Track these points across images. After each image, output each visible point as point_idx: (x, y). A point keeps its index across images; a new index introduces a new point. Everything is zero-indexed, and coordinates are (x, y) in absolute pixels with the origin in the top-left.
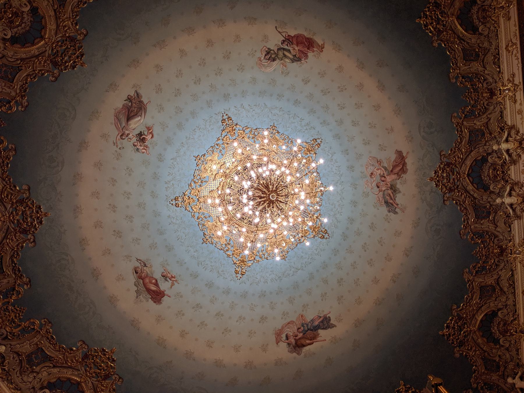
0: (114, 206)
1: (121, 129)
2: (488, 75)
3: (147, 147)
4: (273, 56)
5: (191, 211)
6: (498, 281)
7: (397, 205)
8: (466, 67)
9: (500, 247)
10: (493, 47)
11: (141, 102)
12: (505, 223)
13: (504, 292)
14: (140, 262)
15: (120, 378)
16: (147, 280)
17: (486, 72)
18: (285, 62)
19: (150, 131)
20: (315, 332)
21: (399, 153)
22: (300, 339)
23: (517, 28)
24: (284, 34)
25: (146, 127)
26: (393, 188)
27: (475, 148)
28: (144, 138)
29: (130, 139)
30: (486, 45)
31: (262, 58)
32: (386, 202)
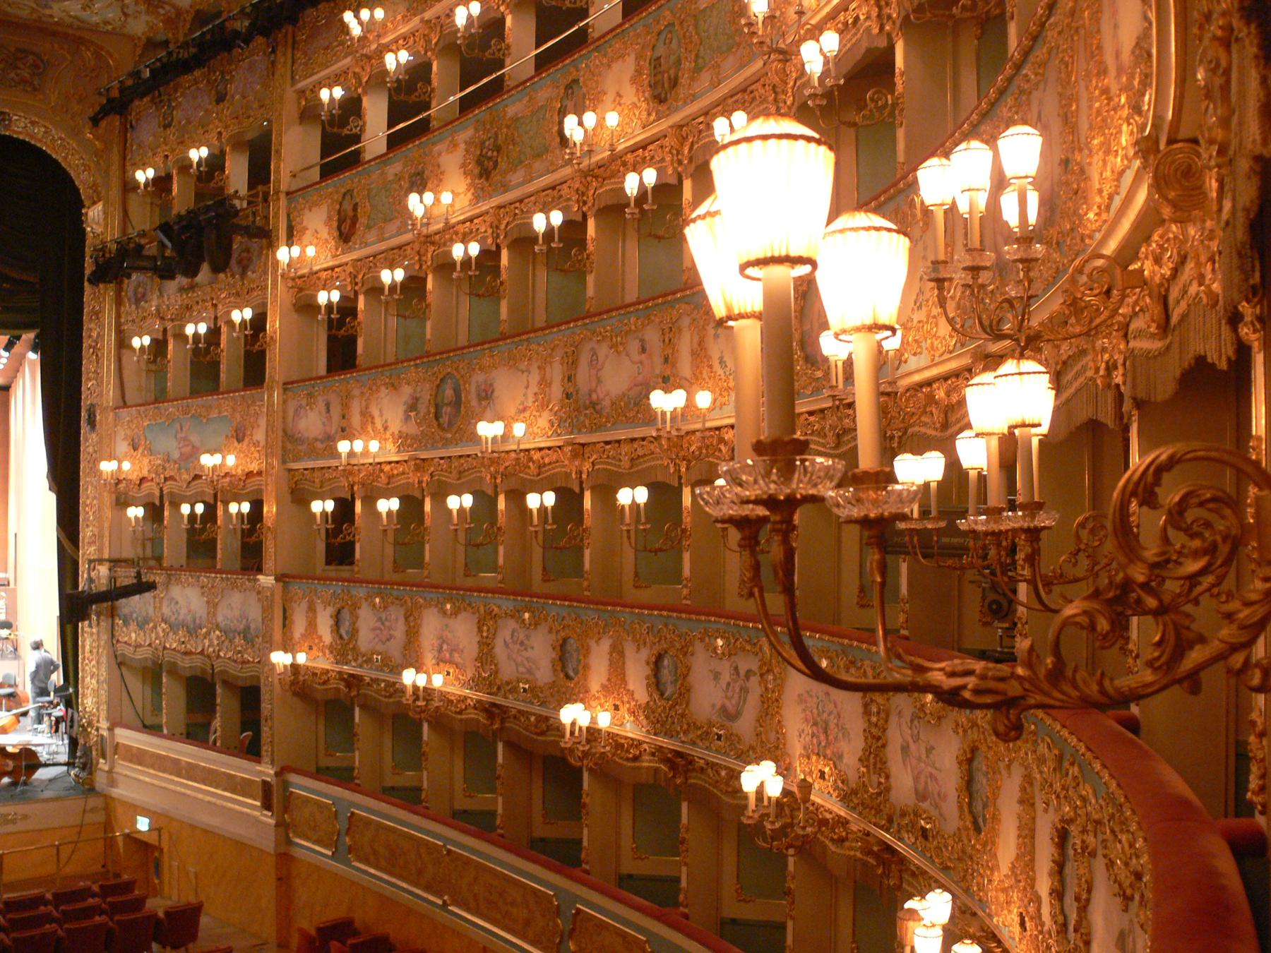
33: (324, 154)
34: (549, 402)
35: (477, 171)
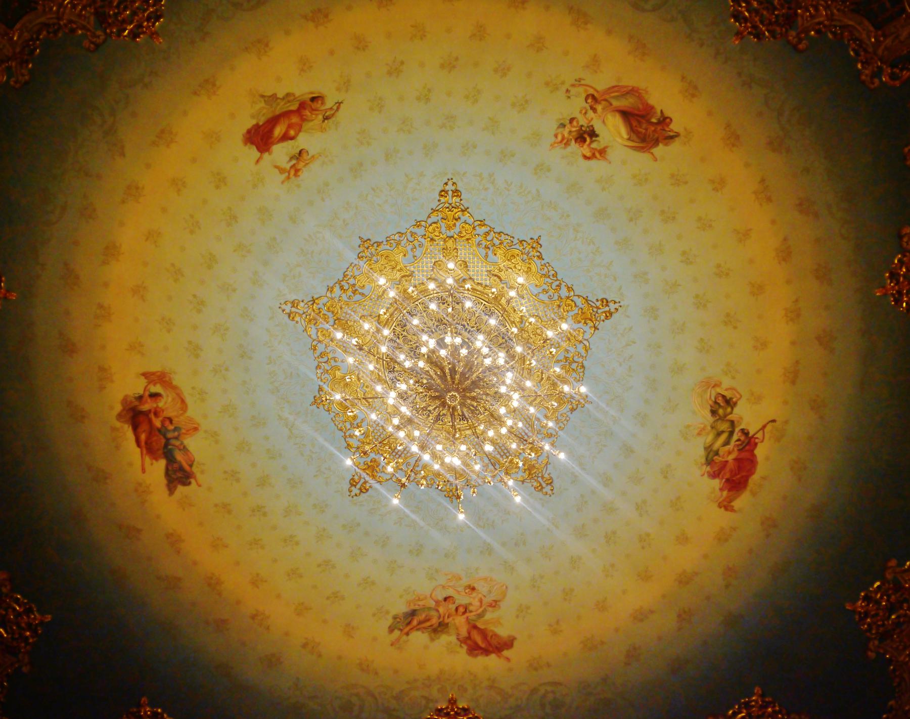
0: (454, 67)
1: (607, 97)
3: (567, 144)
4: (721, 411)
5: (430, 221)
7: (407, 634)
11: (656, 143)
14: (335, 108)
15: (97, 46)
16: (295, 119)
18: (708, 434)
19: (597, 155)
20: (160, 452)
21: (508, 644)
22: (150, 422)
24: (759, 435)
25: (606, 147)
26: (441, 628)
28: (585, 141)
29: (586, 113)
31: (719, 390)
32: (413, 613)
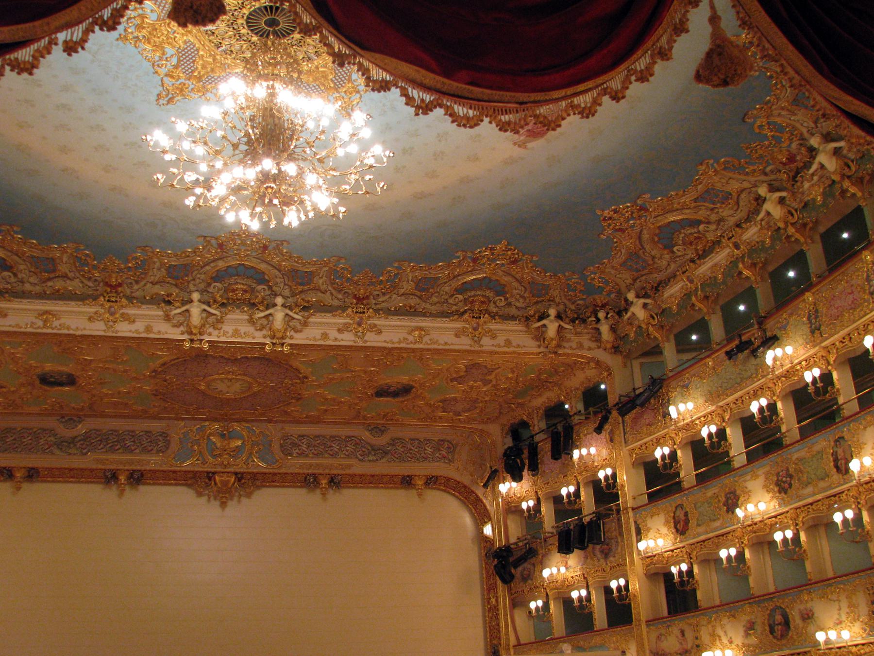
2: (390, 298)
6: (65, 277)
8: (410, 278)
9: (120, 285)
10: (428, 306)
12: (157, 294)
13: (44, 282)
17: (395, 296)
23: (441, 347)
27: (283, 274)
30: (435, 299)
33: (649, 485)
34: (859, 616)
35: (776, 489)
